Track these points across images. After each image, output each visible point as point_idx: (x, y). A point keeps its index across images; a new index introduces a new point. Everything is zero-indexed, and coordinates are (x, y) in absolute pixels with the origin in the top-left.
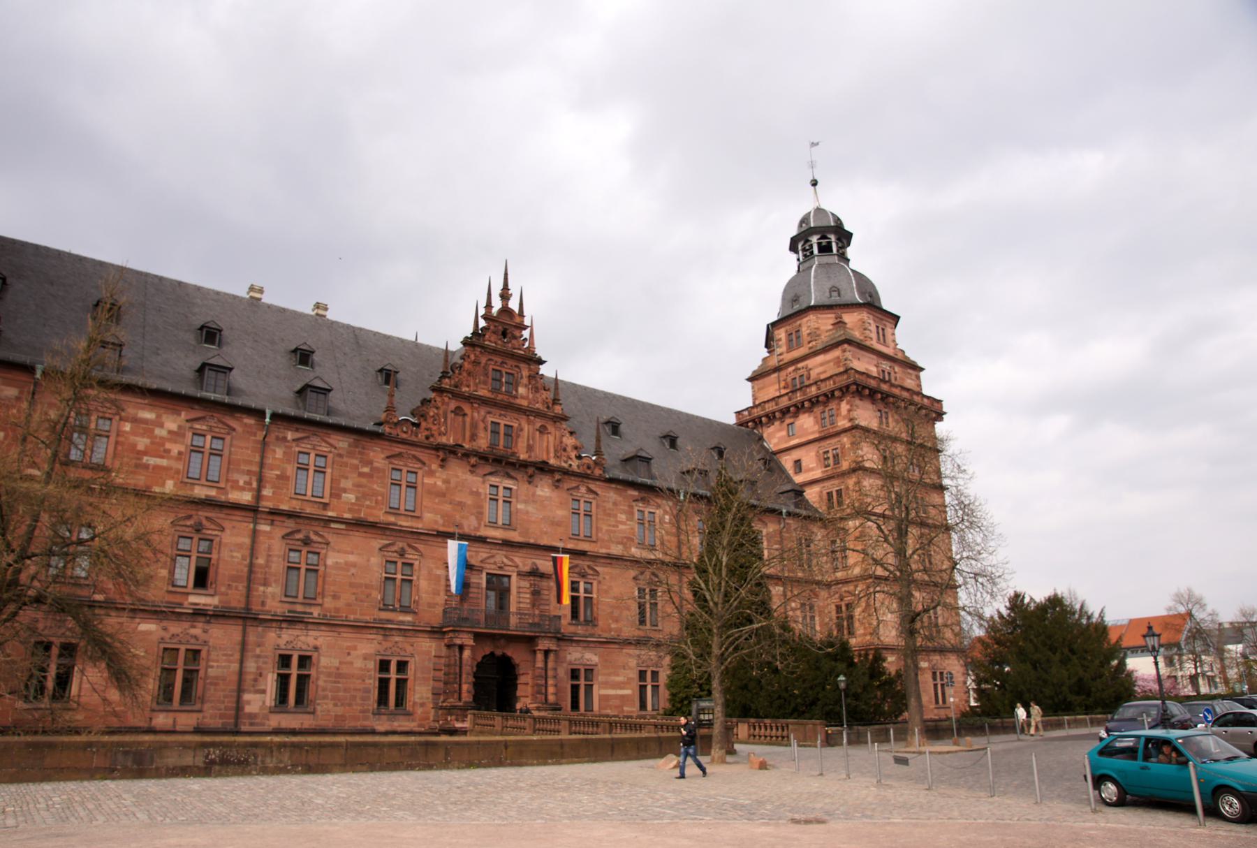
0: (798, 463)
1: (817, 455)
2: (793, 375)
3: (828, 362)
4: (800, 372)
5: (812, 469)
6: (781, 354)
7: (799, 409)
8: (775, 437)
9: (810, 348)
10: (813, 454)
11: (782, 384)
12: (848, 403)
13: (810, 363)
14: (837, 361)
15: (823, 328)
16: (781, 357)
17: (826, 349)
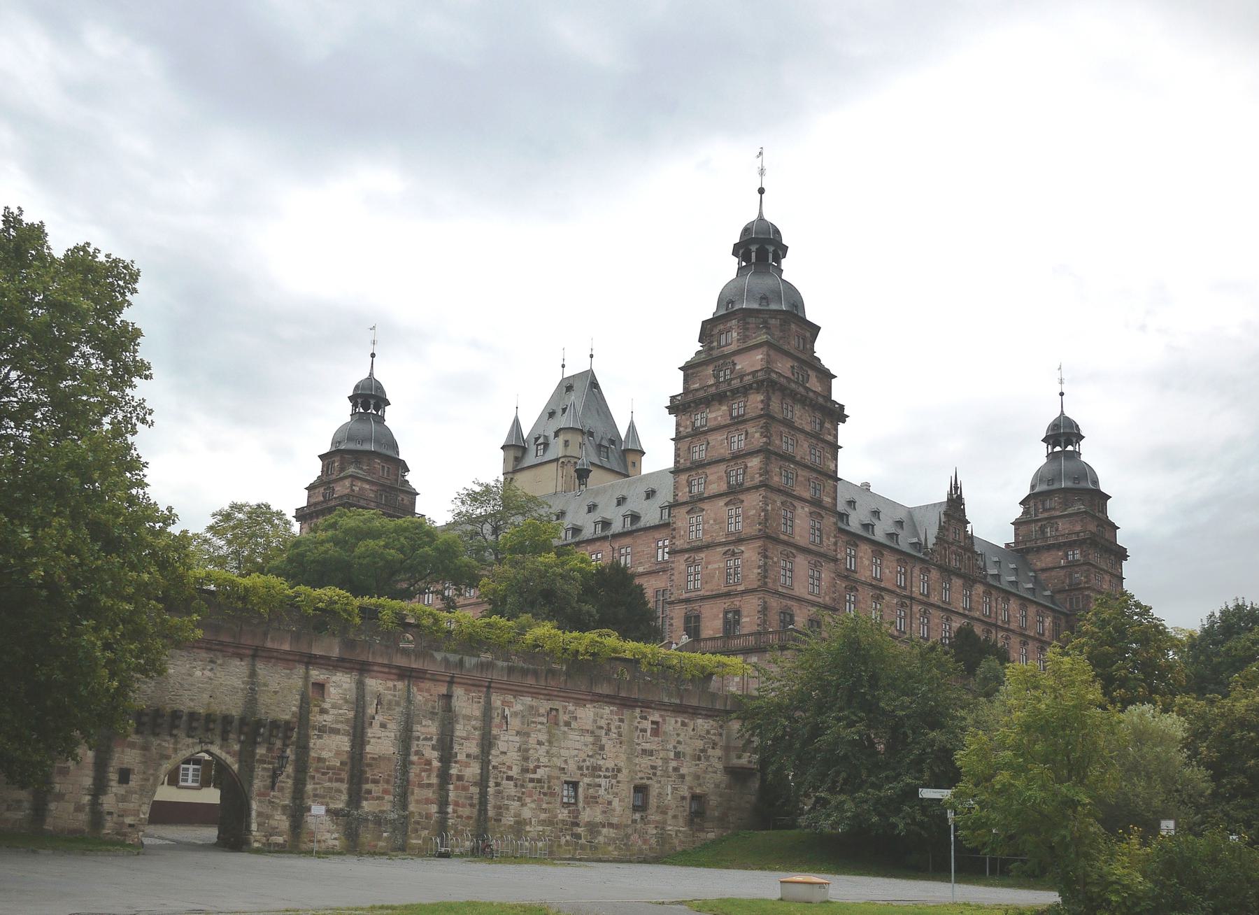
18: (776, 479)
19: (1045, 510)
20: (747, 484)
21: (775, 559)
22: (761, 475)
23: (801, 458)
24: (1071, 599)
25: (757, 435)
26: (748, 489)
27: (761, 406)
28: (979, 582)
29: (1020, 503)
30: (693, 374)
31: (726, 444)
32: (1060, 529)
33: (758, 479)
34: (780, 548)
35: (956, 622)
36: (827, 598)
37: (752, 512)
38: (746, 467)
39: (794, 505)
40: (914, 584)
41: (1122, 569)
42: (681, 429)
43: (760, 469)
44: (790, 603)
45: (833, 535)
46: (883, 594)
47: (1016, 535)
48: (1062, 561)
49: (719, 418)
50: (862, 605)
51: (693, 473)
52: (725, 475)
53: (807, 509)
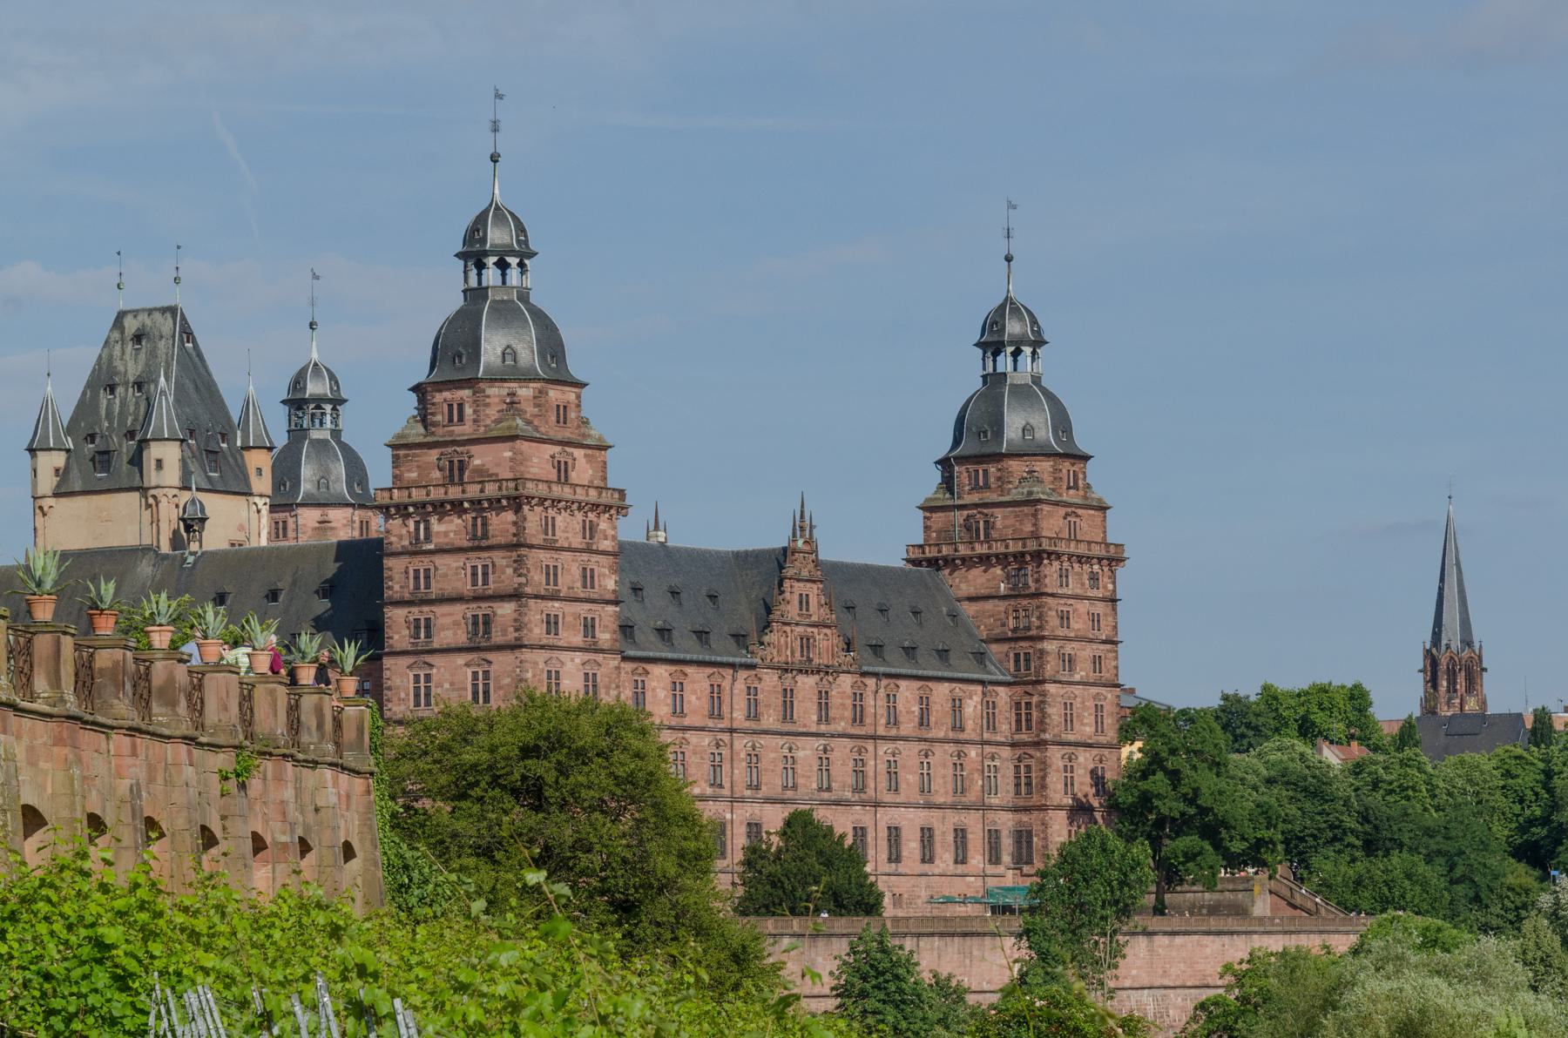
18: (537, 631)
19: (976, 488)
20: (498, 639)
22: (517, 630)
23: (569, 588)
24: (1017, 656)
25: (509, 571)
26: (500, 648)
27: (513, 530)
28: (844, 672)
29: (936, 463)
30: (407, 456)
31: (463, 576)
32: (999, 524)
33: (511, 636)
35: (804, 749)
37: (507, 681)
38: (495, 614)
40: (735, 707)
41: (1114, 583)
42: (393, 539)
43: (516, 620)
45: (613, 686)
46: (688, 735)
47: (927, 528)
48: (1002, 585)
49: (452, 535)
51: (415, 610)
52: (463, 621)
53: (578, 661)
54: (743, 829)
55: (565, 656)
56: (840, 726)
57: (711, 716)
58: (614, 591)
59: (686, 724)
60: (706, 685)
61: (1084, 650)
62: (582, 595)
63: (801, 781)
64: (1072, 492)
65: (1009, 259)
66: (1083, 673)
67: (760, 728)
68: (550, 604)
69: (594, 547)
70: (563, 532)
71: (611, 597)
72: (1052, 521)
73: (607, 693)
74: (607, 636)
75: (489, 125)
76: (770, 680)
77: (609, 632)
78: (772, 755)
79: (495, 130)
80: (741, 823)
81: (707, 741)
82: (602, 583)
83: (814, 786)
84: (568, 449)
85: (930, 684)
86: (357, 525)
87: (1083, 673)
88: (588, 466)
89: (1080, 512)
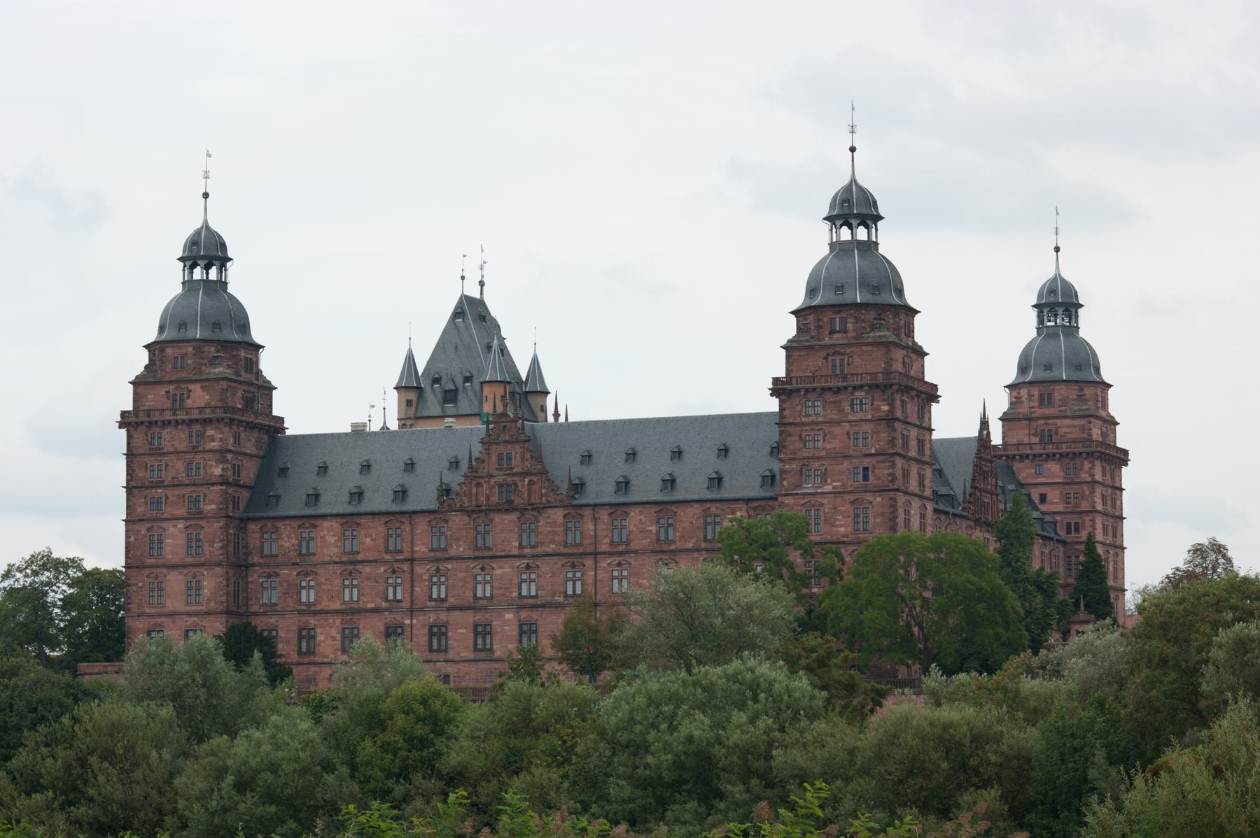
0: (1043, 498)
1: (1061, 493)
2: (1042, 427)
3: (1075, 426)
4: (1050, 427)
5: (1056, 503)
6: (1033, 407)
7: (1050, 457)
8: (1025, 472)
9: (1060, 411)
10: (1057, 492)
11: (1033, 431)
12: (1090, 462)
13: (1060, 422)
14: (1083, 428)
15: (1070, 397)
16: (1033, 410)
17: (1074, 417)
21: (140, 584)
34: (147, 572)
36: (212, 604)
39: (162, 528)
44: (159, 620)
46: (358, 567)
50: (329, 587)
53: (181, 526)
54: (426, 630)
55: (165, 525)
56: (551, 548)
57: (387, 551)
58: (221, 476)
59: (359, 559)
60: (382, 529)
61: (842, 464)
62: (187, 482)
63: (495, 592)
64: (836, 336)
65: (853, 149)
66: (839, 484)
67: (447, 556)
68: (154, 491)
69: (201, 448)
70: (169, 441)
71: (220, 480)
72: (806, 363)
73: (212, 546)
74: (213, 507)
75: (202, 174)
76: (457, 521)
77: (216, 504)
78: (460, 575)
79: (206, 177)
80: (423, 626)
81: (382, 569)
82: (209, 471)
83: (515, 594)
84: (183, 386)
85: (673, 508)
86: (1036, 397)
87: (839, 484)
88: (205, 393)
89: (848, 350)
